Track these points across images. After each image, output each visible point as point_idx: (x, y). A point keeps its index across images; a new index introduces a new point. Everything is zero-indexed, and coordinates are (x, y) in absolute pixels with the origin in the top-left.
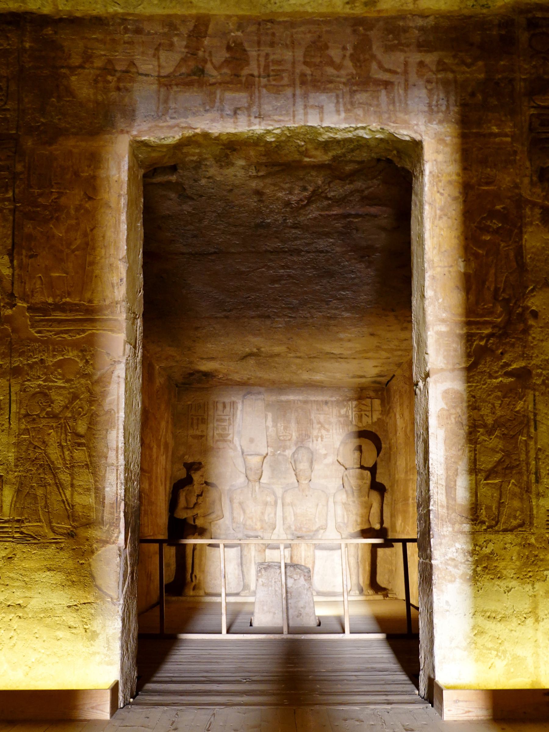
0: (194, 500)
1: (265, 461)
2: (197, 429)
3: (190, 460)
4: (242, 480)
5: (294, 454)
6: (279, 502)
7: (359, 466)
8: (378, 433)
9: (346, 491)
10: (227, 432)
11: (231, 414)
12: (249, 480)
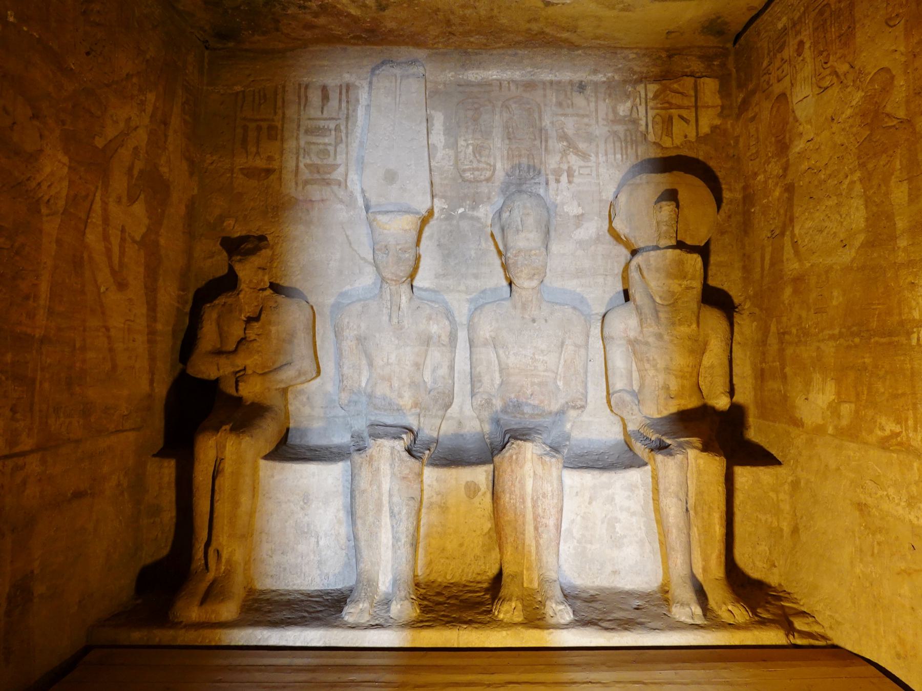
0: (236, 331)
2: (258, 153)
3: (238, 231)
4: (367, 279)
5: (500, 213)
6: (462, 335)
7: (674, 243)
8: (712, 164)
9: (637, 307)
10: (330, 161)
11: (342, 115)
12: (383, 280)
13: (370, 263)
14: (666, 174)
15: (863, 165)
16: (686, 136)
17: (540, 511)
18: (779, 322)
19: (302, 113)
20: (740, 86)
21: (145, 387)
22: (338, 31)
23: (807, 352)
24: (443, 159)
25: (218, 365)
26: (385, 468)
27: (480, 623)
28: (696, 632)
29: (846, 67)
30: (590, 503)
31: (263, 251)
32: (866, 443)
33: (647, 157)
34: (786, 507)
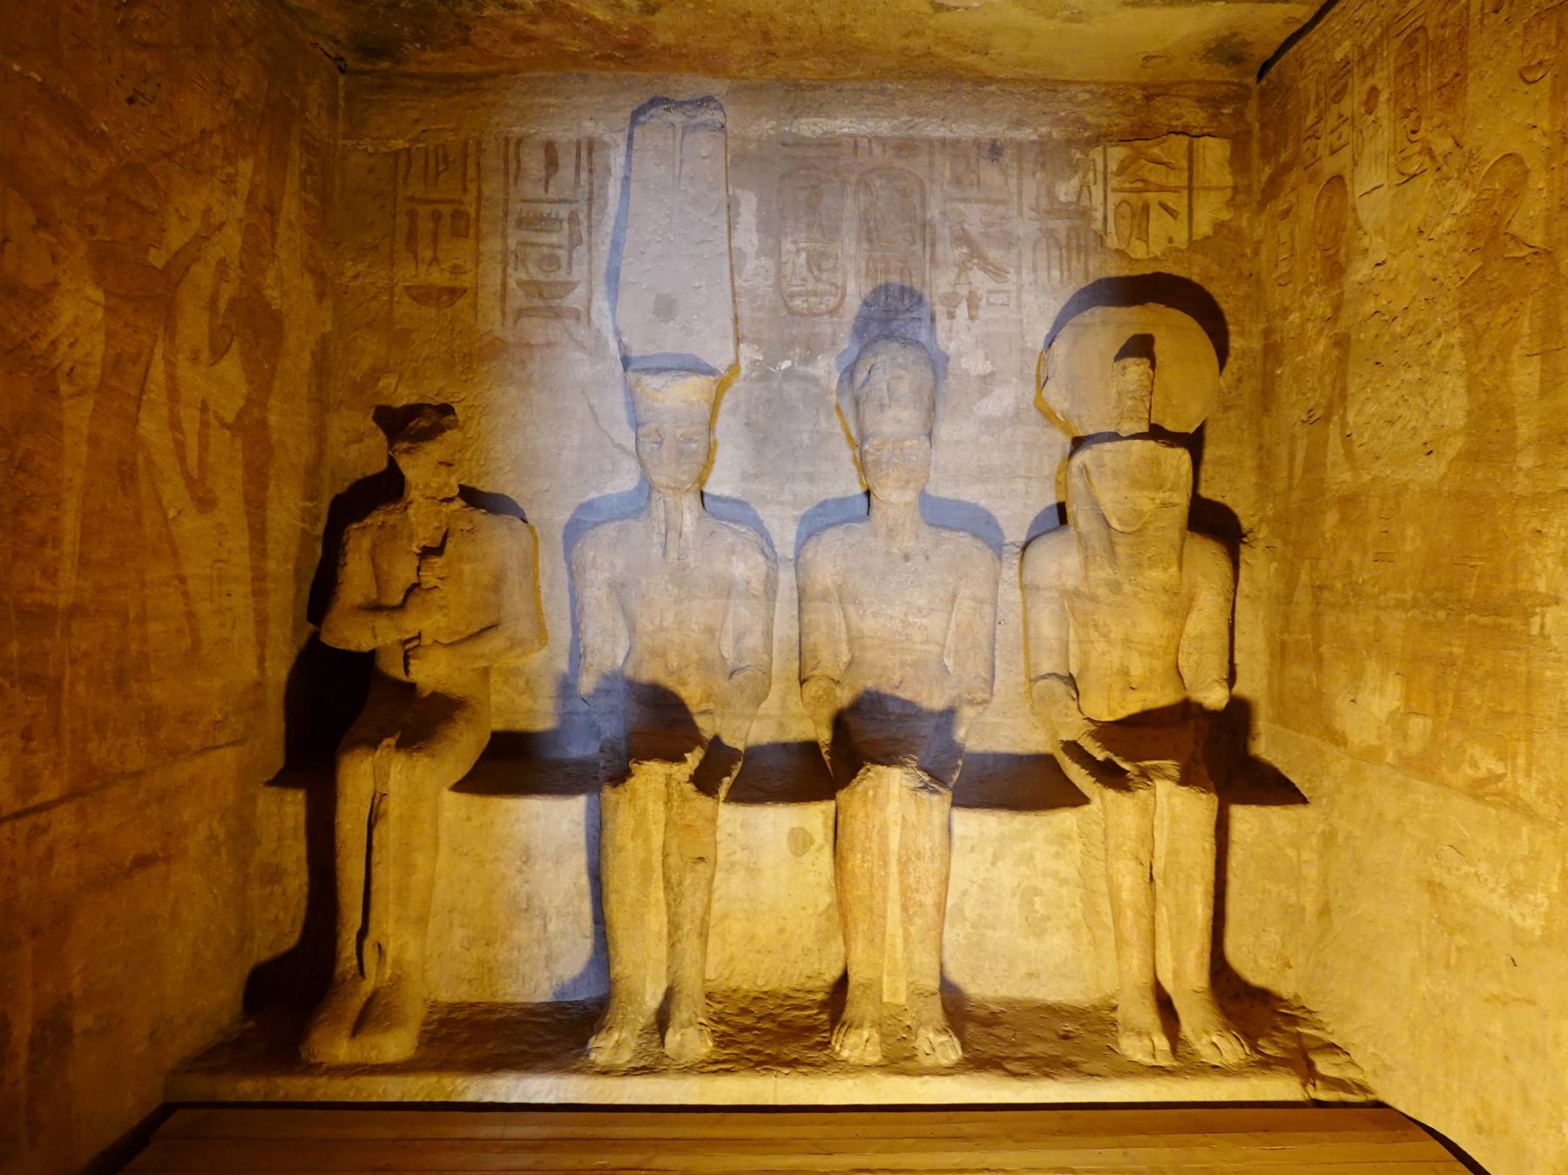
0: (404, 571)
1: (726, 404)
2: (435, 259)
3: (404, 397)
5: (850, 372)
7: (1143, 428)
8: (1213, 289)
9: (1080, 536)
10: (561, 275)
13: (629, 453)
14: (1136, 309)
15: (1467, 320)
16: (1171, 240)
17: (912, 881)
18: (1314, 568)
19: (512, 190)
20: (1266, 155)
21: (250, 671)
22: (574, 46)
23: (1358, 625)
24: (756, 275)
25: (373, 629)
26: (656, 812)
27: (810, 1065)
28: (1159, 1080)
29: (1448, 144)
30: (994, 863)
31: (449, 432)
32: (1448, 786)
33: (1103, 275)
34: (1312, 873)
